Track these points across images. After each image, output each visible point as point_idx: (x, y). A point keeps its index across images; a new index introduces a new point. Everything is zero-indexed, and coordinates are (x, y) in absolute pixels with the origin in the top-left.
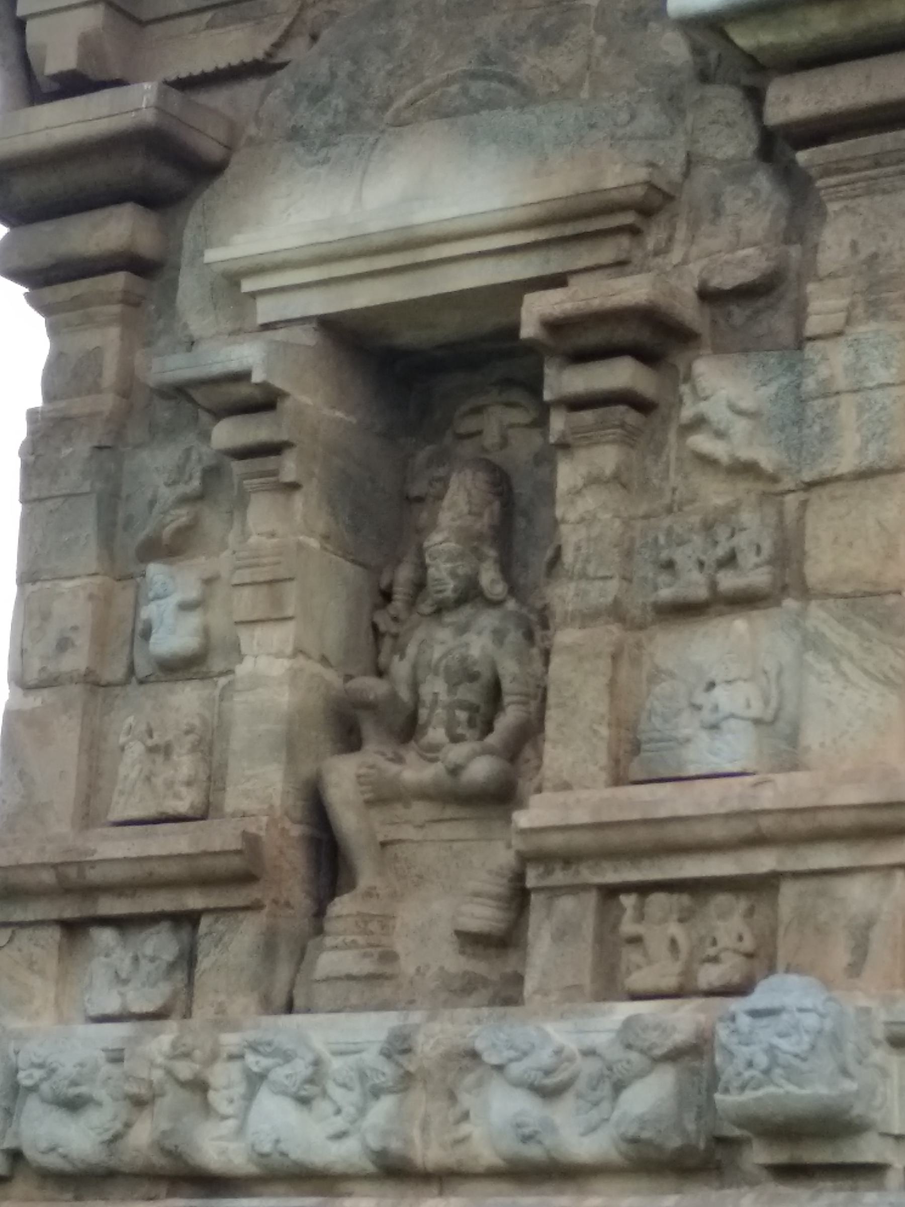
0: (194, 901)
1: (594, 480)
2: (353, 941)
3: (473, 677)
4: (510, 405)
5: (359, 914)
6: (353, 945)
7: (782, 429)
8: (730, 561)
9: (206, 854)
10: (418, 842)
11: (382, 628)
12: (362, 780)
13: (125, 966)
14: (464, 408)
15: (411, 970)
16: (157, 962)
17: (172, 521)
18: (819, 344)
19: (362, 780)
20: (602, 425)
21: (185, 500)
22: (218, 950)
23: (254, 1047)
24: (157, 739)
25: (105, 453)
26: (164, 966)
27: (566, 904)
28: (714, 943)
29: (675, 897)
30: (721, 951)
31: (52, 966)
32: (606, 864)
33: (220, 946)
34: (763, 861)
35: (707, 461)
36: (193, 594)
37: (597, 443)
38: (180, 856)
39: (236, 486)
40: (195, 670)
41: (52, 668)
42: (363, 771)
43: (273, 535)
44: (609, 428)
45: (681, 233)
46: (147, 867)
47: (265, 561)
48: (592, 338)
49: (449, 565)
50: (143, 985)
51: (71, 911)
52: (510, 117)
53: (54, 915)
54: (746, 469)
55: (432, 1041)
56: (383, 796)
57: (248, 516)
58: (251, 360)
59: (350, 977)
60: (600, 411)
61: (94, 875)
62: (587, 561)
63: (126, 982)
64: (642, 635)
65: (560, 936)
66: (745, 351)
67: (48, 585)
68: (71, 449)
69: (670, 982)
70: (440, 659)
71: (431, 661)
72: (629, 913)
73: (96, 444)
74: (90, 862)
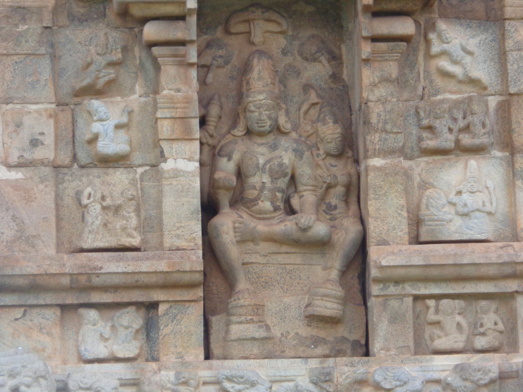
1: (386, 80)
2: (252, 319)
4: (269, 20)
5: (255, 305)
6: (252, 321)
7: (485, 62)
8: (467, 129)
9: (178, 271)
13: (107, 332)
15: (279, 335)
16: (130, 329)
17: (104, 76)
18: (512, 22)
19: (237, 230)
20: (392, 51)
21: (111, 64)
23: (229, 379)
24: (108, 202)
25: (48, 30)
26: (134, 330)
27: (394, 303)
28: (482, 325)
29: (457, 302)
30: (487, 330)
31: (56, 331)
32: (420, 284)
34: (512, 286)
35: (446, 75)
36: (124, 119)
38: (161, 272)
39: (138, 58)
40: (122, 163)
41: (28, 156)
43: (178, 90)
44: (394, 53)
46: (137, 277)
47: (179, 105)
49: (267, 112)
50: (123, 342)
51: (71, 299)
53: (60, 302)
54: (473, 82)
55: (344, 376)
56: (246, 238)
59: (253, 339)
61: (96, 281)
62: (385, 122)
63: (106, 340)
66: (458, 18)
67: (19, 106)
68: (26, 27)
69: (460, 345)
70: (265, 164)
71: (258, 164)
72: (432, 310)
73: (45, 25)
74: (96, 273)
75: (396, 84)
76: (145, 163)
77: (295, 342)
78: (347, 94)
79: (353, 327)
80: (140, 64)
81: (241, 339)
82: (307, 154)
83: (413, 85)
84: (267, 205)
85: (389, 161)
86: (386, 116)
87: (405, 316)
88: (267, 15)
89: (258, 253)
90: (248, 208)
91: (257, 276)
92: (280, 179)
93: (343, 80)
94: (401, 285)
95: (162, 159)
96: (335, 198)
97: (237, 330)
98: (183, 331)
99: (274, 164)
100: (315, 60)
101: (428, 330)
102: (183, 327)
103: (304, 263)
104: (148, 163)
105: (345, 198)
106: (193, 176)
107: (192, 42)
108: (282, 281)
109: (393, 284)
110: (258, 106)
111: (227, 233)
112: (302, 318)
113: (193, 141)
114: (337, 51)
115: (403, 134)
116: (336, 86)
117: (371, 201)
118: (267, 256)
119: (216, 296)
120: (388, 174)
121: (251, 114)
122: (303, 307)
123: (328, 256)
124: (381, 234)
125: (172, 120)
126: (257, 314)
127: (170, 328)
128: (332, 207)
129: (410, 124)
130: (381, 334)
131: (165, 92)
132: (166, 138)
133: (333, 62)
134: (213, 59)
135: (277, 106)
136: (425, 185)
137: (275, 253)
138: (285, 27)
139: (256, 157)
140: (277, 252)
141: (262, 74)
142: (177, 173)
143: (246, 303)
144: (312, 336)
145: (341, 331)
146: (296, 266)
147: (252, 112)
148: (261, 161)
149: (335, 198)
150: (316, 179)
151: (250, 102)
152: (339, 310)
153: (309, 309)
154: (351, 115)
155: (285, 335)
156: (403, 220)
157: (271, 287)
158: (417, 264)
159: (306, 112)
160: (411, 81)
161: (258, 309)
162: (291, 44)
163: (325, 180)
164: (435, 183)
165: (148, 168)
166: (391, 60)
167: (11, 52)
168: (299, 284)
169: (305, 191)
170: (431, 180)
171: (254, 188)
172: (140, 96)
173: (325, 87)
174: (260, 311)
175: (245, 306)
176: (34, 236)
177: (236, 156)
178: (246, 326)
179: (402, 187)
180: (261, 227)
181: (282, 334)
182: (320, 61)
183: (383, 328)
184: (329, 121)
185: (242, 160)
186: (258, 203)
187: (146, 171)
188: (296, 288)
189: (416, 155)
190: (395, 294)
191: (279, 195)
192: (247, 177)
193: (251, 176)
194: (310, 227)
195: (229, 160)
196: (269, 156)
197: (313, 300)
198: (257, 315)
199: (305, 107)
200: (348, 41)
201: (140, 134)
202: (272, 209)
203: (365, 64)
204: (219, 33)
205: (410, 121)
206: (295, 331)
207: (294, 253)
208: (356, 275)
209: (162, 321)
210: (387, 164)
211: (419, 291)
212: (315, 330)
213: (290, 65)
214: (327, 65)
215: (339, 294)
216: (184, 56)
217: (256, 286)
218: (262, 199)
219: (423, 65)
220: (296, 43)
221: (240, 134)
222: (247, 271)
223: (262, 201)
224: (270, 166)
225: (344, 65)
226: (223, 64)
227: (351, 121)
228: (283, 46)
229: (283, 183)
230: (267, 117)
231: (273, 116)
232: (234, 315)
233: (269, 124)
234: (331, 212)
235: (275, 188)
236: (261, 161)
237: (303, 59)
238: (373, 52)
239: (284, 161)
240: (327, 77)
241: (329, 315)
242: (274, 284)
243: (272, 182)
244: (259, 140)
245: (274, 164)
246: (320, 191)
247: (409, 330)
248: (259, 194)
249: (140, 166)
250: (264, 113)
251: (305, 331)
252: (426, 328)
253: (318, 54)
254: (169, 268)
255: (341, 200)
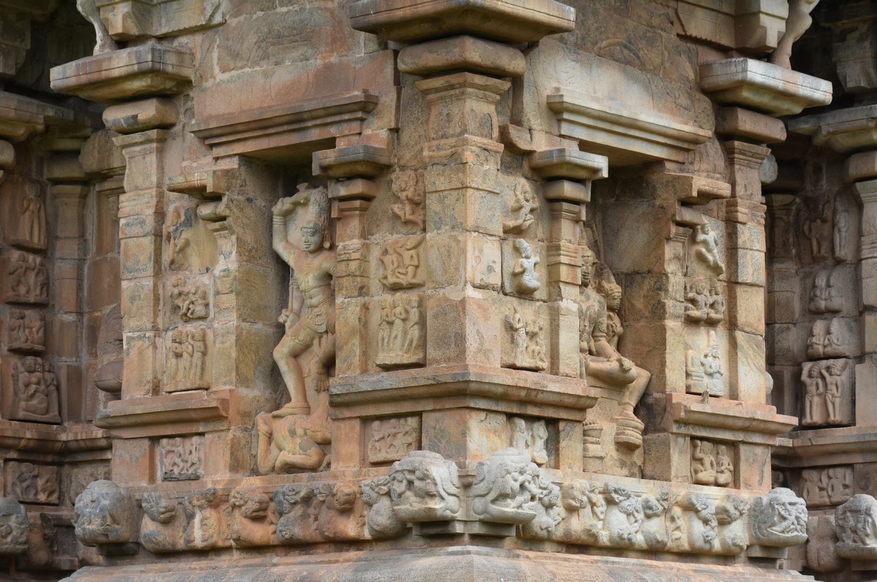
0: (563, 414)
34: (740, 437)
45: (697, 158)
52: (636, 72)
61: (540, 396)
167: (480, 187)
176: (488, 350)
209: (562, 435)
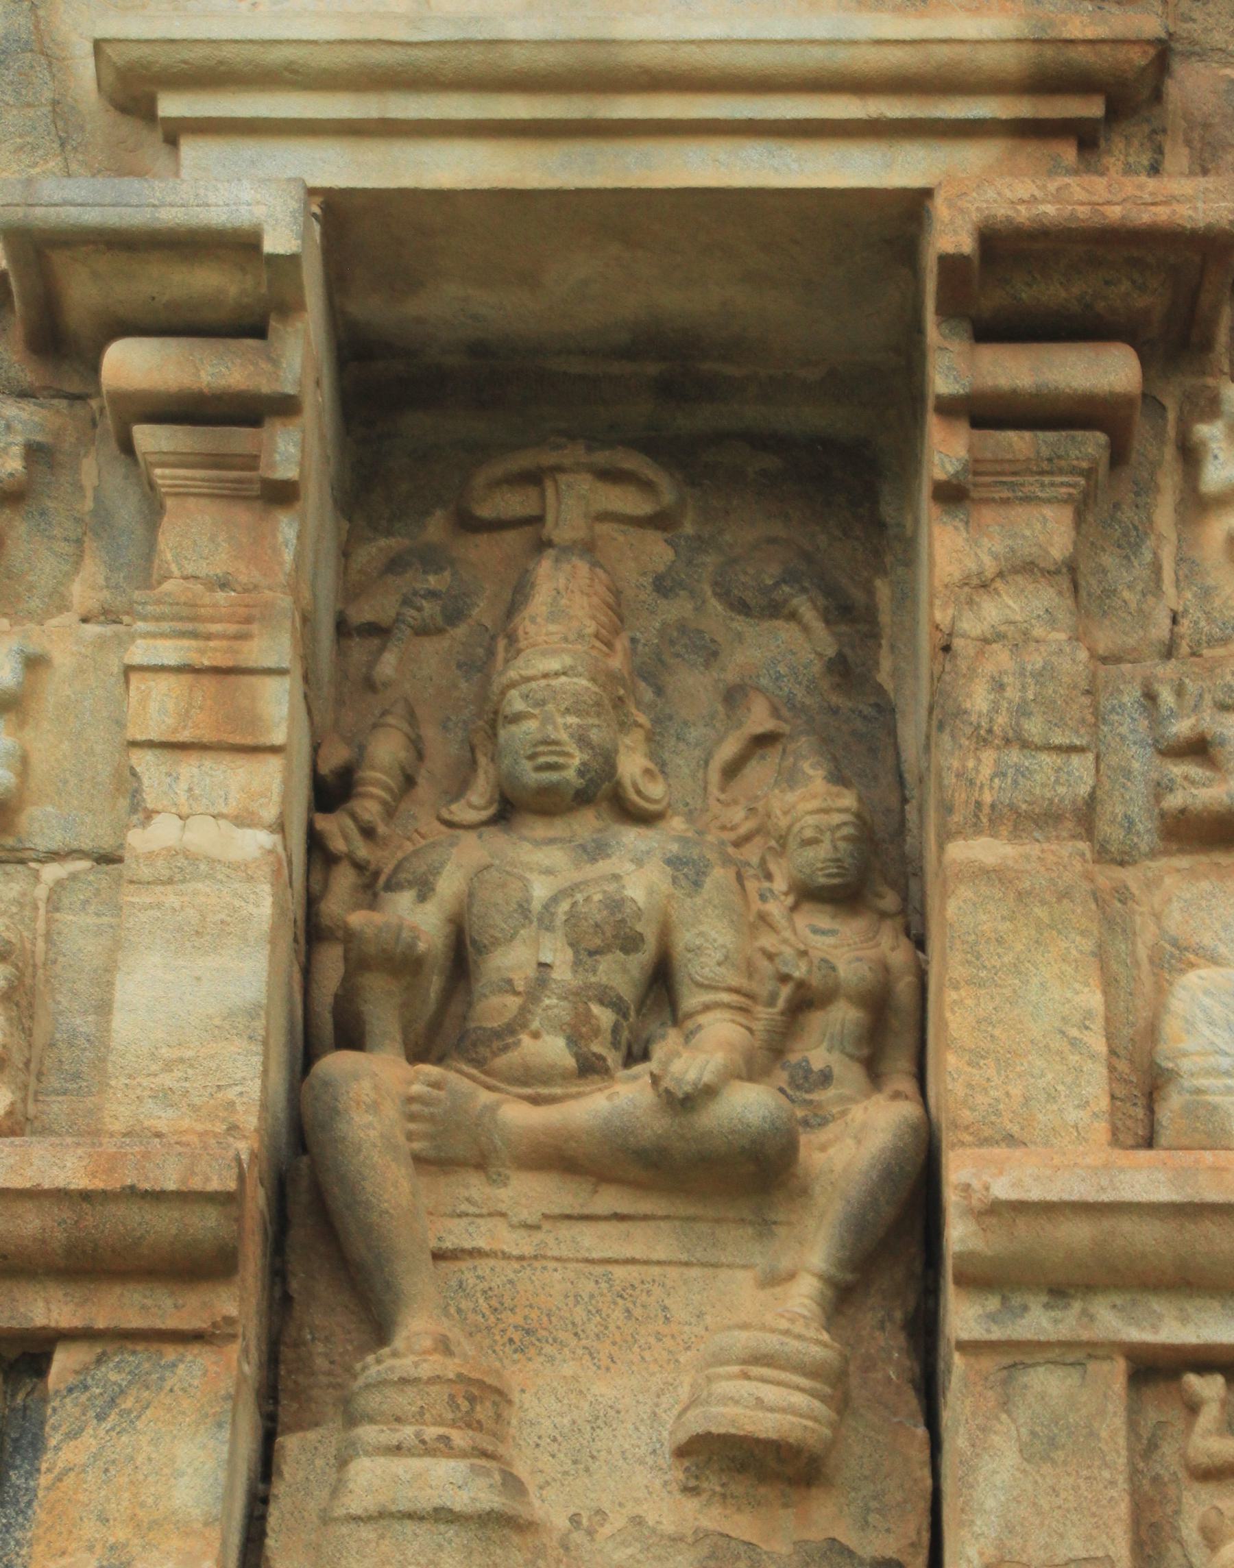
1: (1027, 568)
2: (445, 1439)
3: (630, 943)
5: (461, 1378)
6: (443, 1447)
9: (132, 1193)
10: (521, 1258)
11: (338, 845)
12: (416, 1107)
14: (499, 469)
15: (560, 1521)
19: (416, 1107)
20: (1049, 467)
22: (107, 1425)
27: (1048, 1383)
32: (1157, 1304)
33: (113, 1418)
37: (1028, 500)
38: (61, 1195)
39: (89, 494)
42: (417, 1088)
44: (1061, 472)
48: (1052, 293)
49: (572, 720)
57: (160, 538)
58: (260, 212)
59: (443, 1516)
60: (1051, 436)
62: (1022, 711)
64: (1129, 876)
65: (1041, 1448)
70: (555, 900)
71: (528, 900)
75: (1066, 584)
76: (75, 845)
77: (629, 1551)
78: (893, 732)
79: (874, 1504)
80: (95, 513)
81: (392, 1515)
82: (719, 875)
83: (1133, 606)
84: (553, 1049)
85: (1034, 850)
86: (1024, 688)
87: (1092, 1434)
88: (602, 458)
89: (503, 1215)
90: (479, 1063)
91: (494, 1303)
92: (610, 957)
93: (879, 689)
94: (1077, 1306)
95: (135, 819)
96: (825, 1044)
97: (372, 1479)
98: (140, 1459)
99: (588, 899)
100: (775, 610)
101: (1197, 1505)
102: (144, 1440)
103: (684, 1257)
104: (86, 845)
105: (865, 1052)
106: (250, 879)
107: (285, 407)
108: (592, 1328)
109: (1044, 1298)
110: (539, 696)
111: (374, 1107)
112: (666, 1459)
113: (261, 756)
114: (858, 595)
115: (1091, 756)
116: (850, 704)
117: (956, 988)
118: (537, 1227)
119: (323, 1379)
120: (1029, 893)
121: (514, 728)
122: (669, 1419)
123: (781, 1231)
124: (997, 1113)
125: (186, 679)
126: (471, 1423)
127: (89, 1441)
128: (813, 1078)
129: (1123, 738)
130: (990, 1503)
131: (168, 586)
132: (154, 736)
133: (843, 628)
134: (406, 602)
135: (615, 707)
136: (1176, 956)
137: (568, 1217)
138: (668, 496)
139: (521, 878)
140: (577, 1211)
141: (564, 602)
142: (183, 866)
143: (425, 1371)
144: (701, 1536)
145: (828, 1518)
146: (656, 1271)
147: (517, 718)
148: (540, 890)
149: (825, 1044)
150: (750, 970)
151: (513, 685)
152: (815, 1419)
153: (690, 1414)
154: (905, 801)
155: (585, 1521)
156: (1089, 1066)
157: (548, 1349)
158: (1144, 1198)
159: (732, 770)
160: (1126, 594)
161: (480, 1407)
162: (690, 562)
163: (785, 970)
164: (1222, 949)
165: (85, 864)
166: (1049, 501)
168: (659, 1337)
169: (707, 1008)
170: (1207, 939)
171: (508, 986)
172: (85, 620)
173: (808, 701)
174: (483, 1412)
175: (416, 1381)
177: (449, 885)
178: (417, 1464)
179: (1088, 945)
180: (517, 1115)
181: (575, 1520)
182: (793, 616)
183: (997, 1479)
184: (811, 772)
185: (471, 895)
186: (519, 1041)
187: (74, 877)
188: (647, 1354)
189: (1144, 847)
190: (1053, 1337)
191: (604, 1016)
192: (482, 950)
193: (496, 942)
194: (709, 1092)
195: (422, 898)
196: (569, 875)
197: (709, 1379)
198: (469, 1426)
199: (729, 749)
200: (900, 570)
201: (66, 746)
202: (570, 1062)
203: (947, 512)
204: (435, 528)
205: (1123, 730)
206: (631, 1509)
207: (645, 1218)
208: (898, 1315)
209: (61, 1414)
210: (1027, 858)
211: (1155, 1328)
212: (716, 1511)
213: (682, 627)
214: (818, 626)
215: (817, 1352)
216: (251, 462)
217: (487, 1342)
218: (535, 1025)
219: (1173, 537)
220: (710, 560)
221: (472, 816)
222: (454, 1283)
223: (536, 1035)
224: (574, 904)
225: (884, 642)
226: (440, 620)
227: (903, 822)
228: (662, 569)
229: (621, 973)
230: (572, 736)
231: (594, 735)
232: (372, 1420)
233: (576, 762)
234: (808, 1097)
235: (588, 986)
236: (540, 890)
237: (731, 606)
238: (975, 466)
239: (629, 892)
240: (817, 668)
241: (773, 1435)
242: (561, 1335)
243: (577, 964)
244: (540, 829)
245: (588, 899)
246: (766, 1015)
247: (1113, 1493)
248: (524, 1011)
249: (54, 856)
250: (560, 720)
251: (672, 1511)
252: (1188, 1498)
253: (786, 589)
254: (94, 1175)
255: (851, 1057)
